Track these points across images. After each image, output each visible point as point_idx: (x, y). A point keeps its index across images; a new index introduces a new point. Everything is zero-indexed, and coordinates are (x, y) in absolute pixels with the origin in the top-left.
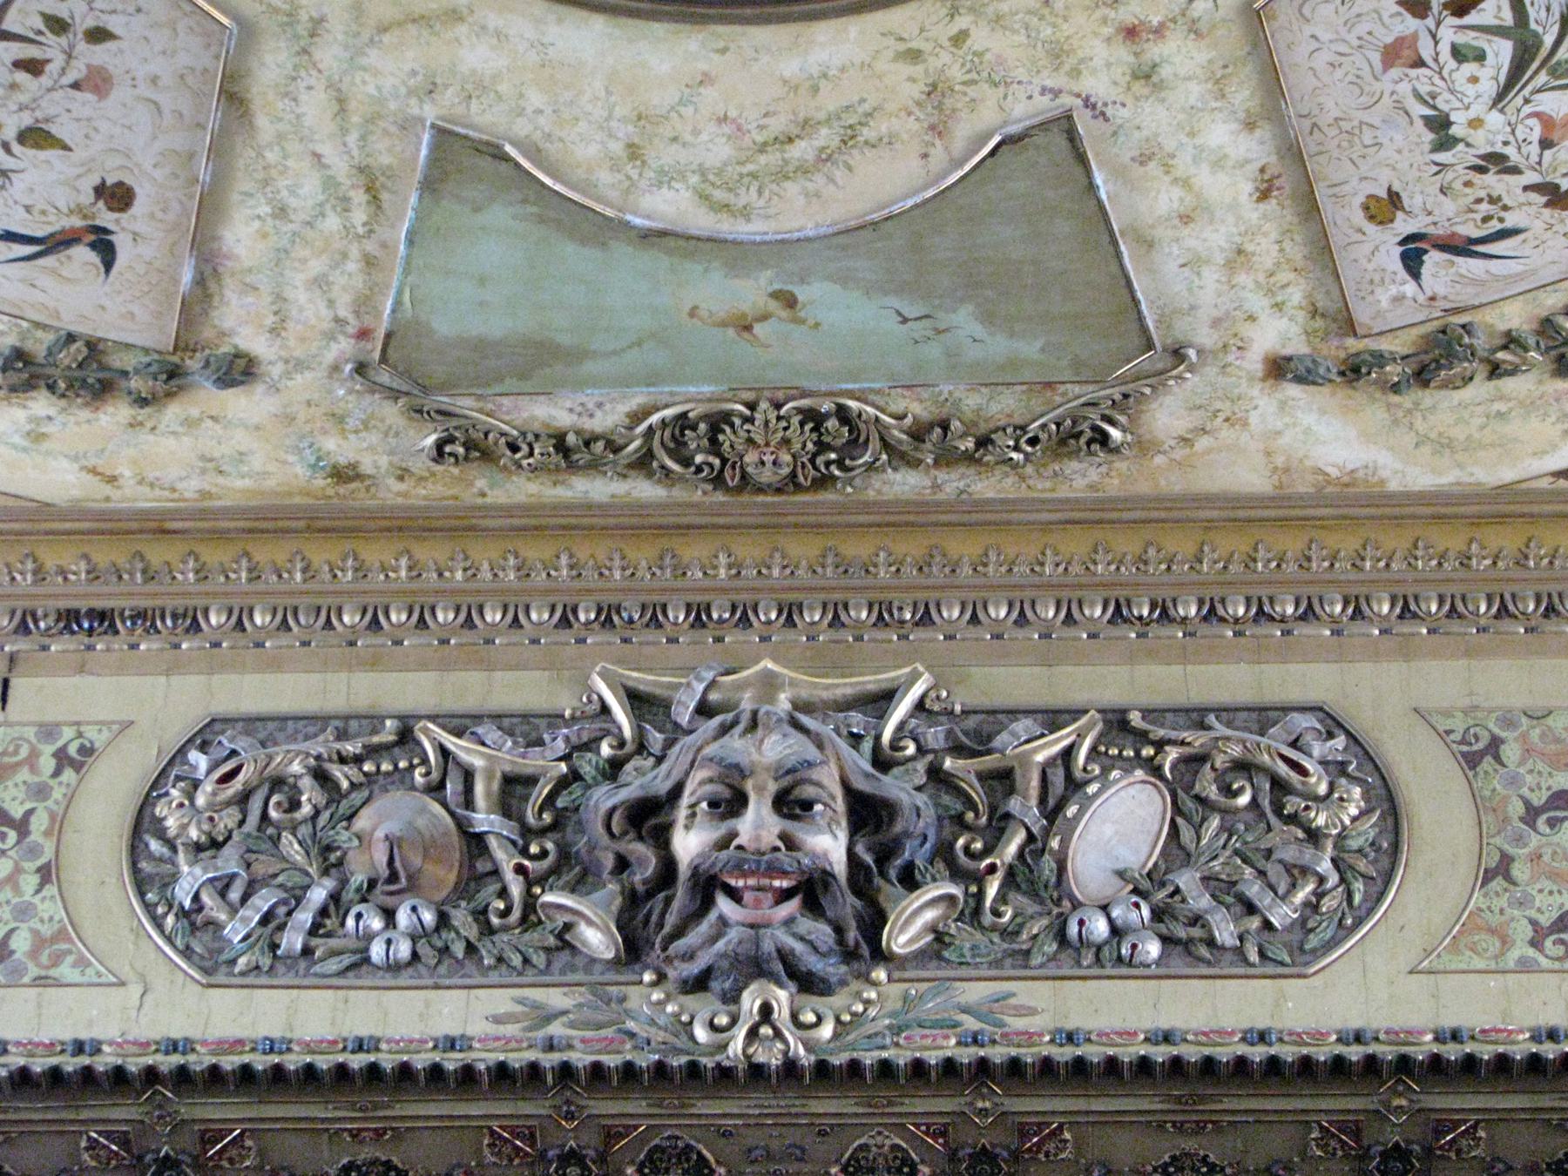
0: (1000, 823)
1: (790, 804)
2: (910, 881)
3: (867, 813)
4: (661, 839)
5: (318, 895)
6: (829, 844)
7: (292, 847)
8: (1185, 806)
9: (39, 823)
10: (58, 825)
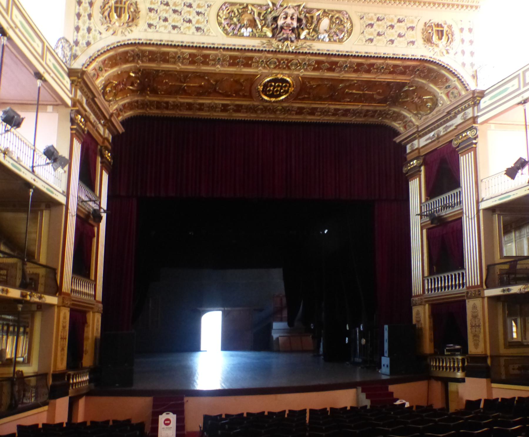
0: (311, 24)
1: (292, 18)
2: (303, 29)
3: (299, 20)
4: (276, 21)
5: (238, 26)
6: (295, 24)
7: (235, 20)
8: (332, 22)
9: (206, 14)
10: (208, 15)
